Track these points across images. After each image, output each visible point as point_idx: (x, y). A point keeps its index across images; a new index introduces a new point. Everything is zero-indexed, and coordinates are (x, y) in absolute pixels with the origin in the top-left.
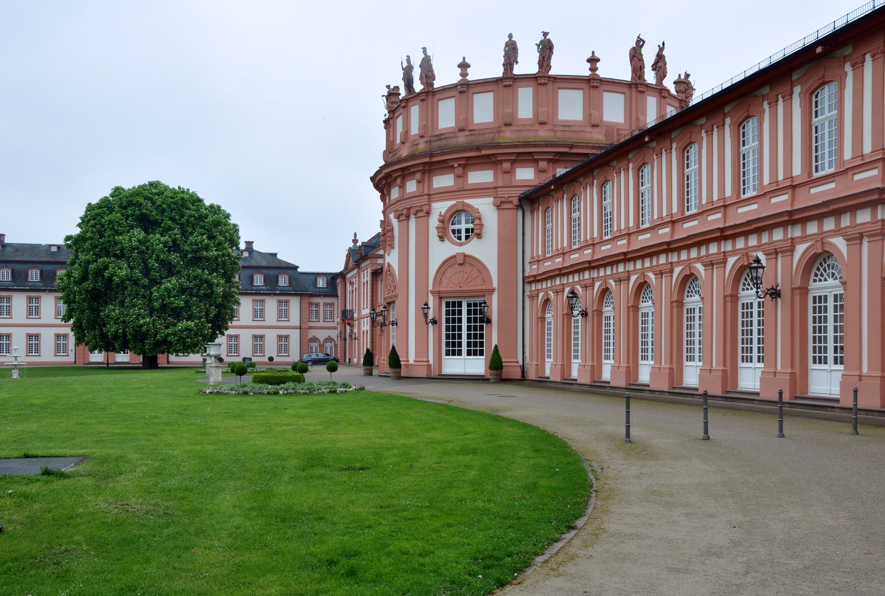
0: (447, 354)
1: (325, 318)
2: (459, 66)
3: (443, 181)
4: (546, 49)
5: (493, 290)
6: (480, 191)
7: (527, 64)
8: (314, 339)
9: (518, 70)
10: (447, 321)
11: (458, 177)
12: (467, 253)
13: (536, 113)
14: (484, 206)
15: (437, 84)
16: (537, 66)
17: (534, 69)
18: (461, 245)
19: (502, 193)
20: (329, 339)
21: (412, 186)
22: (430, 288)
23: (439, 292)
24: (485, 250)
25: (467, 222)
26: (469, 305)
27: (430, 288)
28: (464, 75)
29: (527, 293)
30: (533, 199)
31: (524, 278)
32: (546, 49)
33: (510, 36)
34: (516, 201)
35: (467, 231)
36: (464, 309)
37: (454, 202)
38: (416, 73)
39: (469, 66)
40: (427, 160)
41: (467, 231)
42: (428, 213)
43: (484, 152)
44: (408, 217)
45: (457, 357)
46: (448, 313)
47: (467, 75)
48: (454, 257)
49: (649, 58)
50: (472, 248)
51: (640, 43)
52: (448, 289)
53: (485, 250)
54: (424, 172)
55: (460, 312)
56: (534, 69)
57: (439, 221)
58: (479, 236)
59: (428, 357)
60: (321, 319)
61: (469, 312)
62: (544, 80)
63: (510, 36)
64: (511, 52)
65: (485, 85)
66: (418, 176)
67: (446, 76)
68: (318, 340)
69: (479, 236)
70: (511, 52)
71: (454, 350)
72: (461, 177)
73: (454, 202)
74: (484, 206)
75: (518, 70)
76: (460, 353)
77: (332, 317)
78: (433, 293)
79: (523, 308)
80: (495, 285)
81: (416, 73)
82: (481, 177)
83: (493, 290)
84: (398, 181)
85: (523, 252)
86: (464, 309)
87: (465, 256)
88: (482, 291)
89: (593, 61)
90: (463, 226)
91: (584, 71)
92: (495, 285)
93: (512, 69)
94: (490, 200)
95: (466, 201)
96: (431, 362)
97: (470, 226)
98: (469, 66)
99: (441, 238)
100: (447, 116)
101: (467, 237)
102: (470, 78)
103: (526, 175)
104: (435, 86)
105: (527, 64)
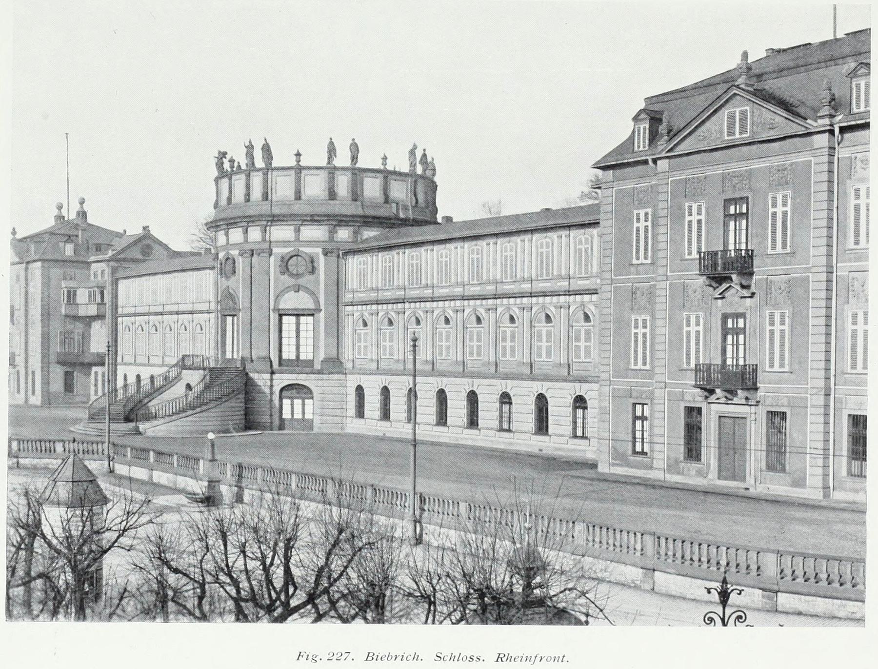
4: (355, 149)
7: (343, 159)
15: (275, 164)
16: (350, 161)
17: (348, 163)
32: (355, 149)
38: (258, 154)
49: (419, 154)
51: (415, 147)
56: (348, 163)
64: (332, 151)
67: (282, 158)
70: (332, 151)
78: (274, 310)
81: (258, 154)
89: (385, 158)
91: (378, 165)
95: (301, 249)
102: (302, 164)
103: (344, 234)
105: (343, 159)
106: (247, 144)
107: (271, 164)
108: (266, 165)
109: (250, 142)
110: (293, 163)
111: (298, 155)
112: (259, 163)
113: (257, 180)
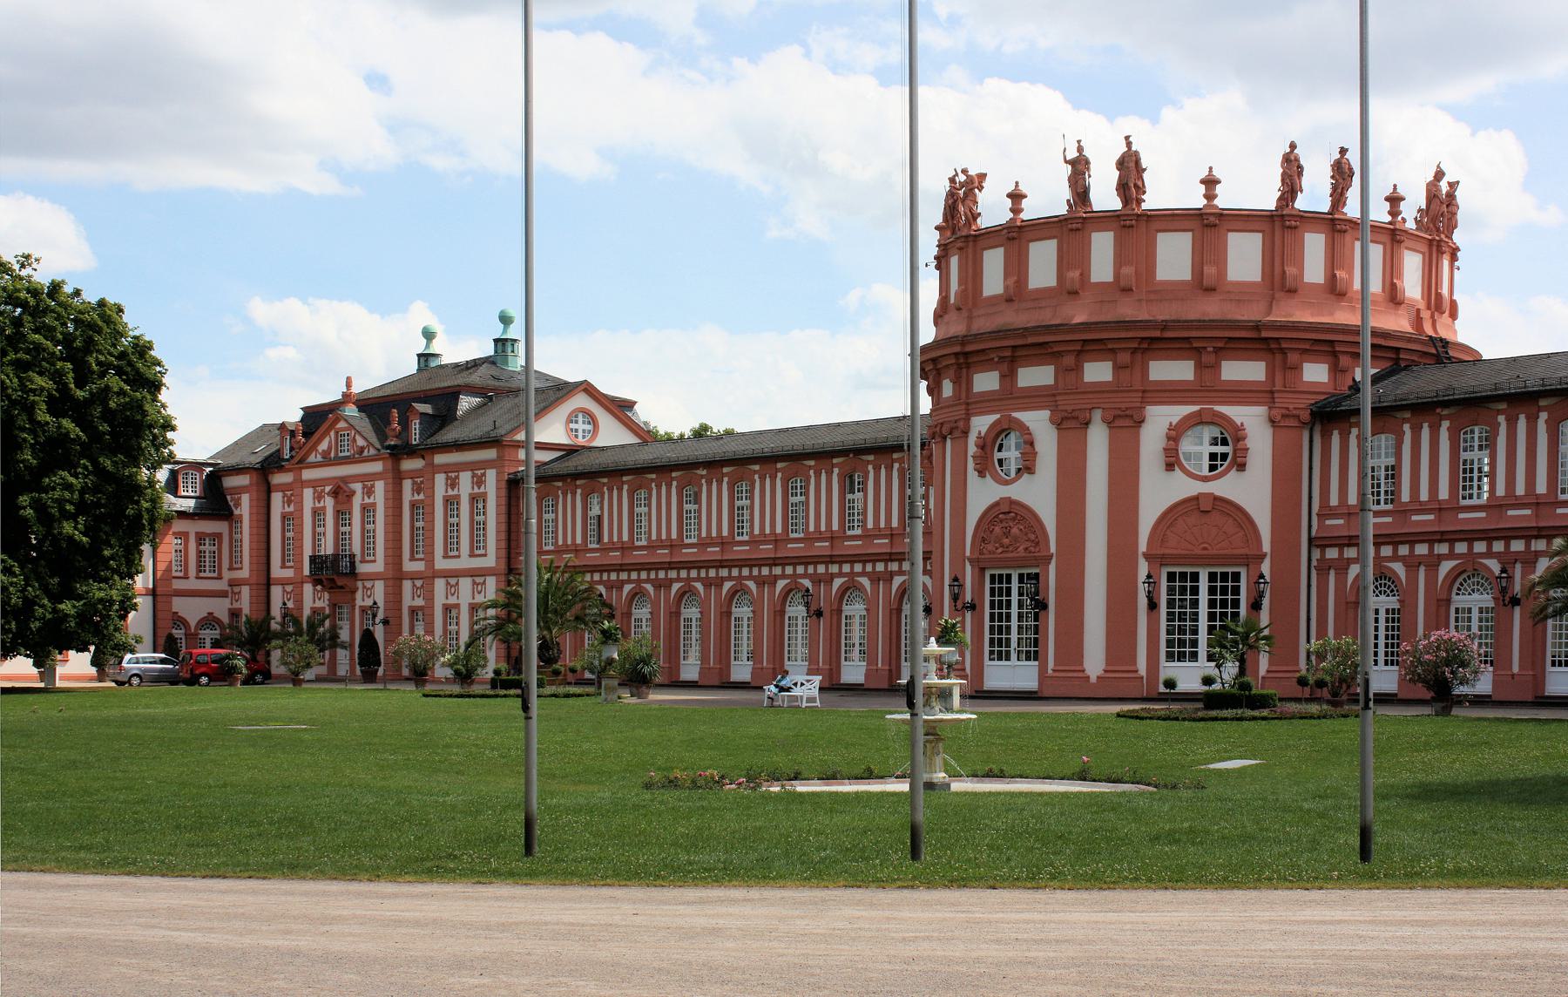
0: (1170, 656)
1: (200, 568)
2: (1202, 182)
3: (1172, 370)
5: (1265, 555)
6: (1242, 393)
7: (1314, 196)
8: (179, 621)
9: (1302, 203)
10: (1171, 603)
11: (1199, 367)
12: (1218, 493)
13: (1332, 278)
14: (1251, 418)
17: (1324, 206)
18: (1205, 479)
19: (1283, 401)
20: (209, 621)
21: (1098, 372)
22: (1143, 546)
23: (1163, 556)
24: (1252, 490)
25: (1214, 442)
26: (1212, 577)
27: (1143, 546)
28: (1210, 196)
29: (1314, 563)
30: (1331, 415)
31: (1310, 540)
32: (1341, 173)
33: (1293, 146)
34: (1305, 416)
35: (1213, 456)
36: (1203, 585)
37: (1195, 408)
39: (1218, 182)
40: (1157, 334)
41: (1213, 456)
42: (1140, 422)
43: (1264, 334)
44: (1087, 424)
45: (1188, 664)
46: (1171, 590)
47: (1215, 196)
48: (1196, 498)
50: (1228, 487)
52: (1180, 552)
53: (1252, 490)
54: (1134, 351)
55: (1195, 591)
57: (1169, 438)
58: (1242, 467)
59: (1134, 663)
60: (192, 571)
61: (1212, 591)
62: (1334, 224)
63: (1293, 146)
65: (1245, 220)
66: (1124, 358)
68: (185, 623)
69: (1242, 467)
71: (1182, 650)
72: (1208, 368)
73: (1195, 408)
74: (1251, 418)
75: (1302, 203)
76: (1194, 656)
77: (217, 566)
78: (1147, 556)
79: (1309, 586)
80: (1266, 547)
82: (1248, 371)
83: (1265, 555)
84: (1069, 360)
85: (1310, 498)
86: (1203, 585)
87: (1217, 499)
88: (1247, 556)
90: (1208, 449)
92: (1266, 547)
93: (1294, 199)
94: (1261, 410)
96: (1143, 671)
97: (1219, 449)
98: (1218, 182)
99: (1170, 467)
100: (1174, 258)
101: (1212, 468)
103: (1316, 373)
104: (1144, 206)
105: (1314, 196)
106: (1072, 154)
107: (1139, 201)
108: (1126, 201)
109: (1080, 149)
110: (1195, 199)
111: (1210, 183)
112: (1105, 197)
113: (1102, 246)
